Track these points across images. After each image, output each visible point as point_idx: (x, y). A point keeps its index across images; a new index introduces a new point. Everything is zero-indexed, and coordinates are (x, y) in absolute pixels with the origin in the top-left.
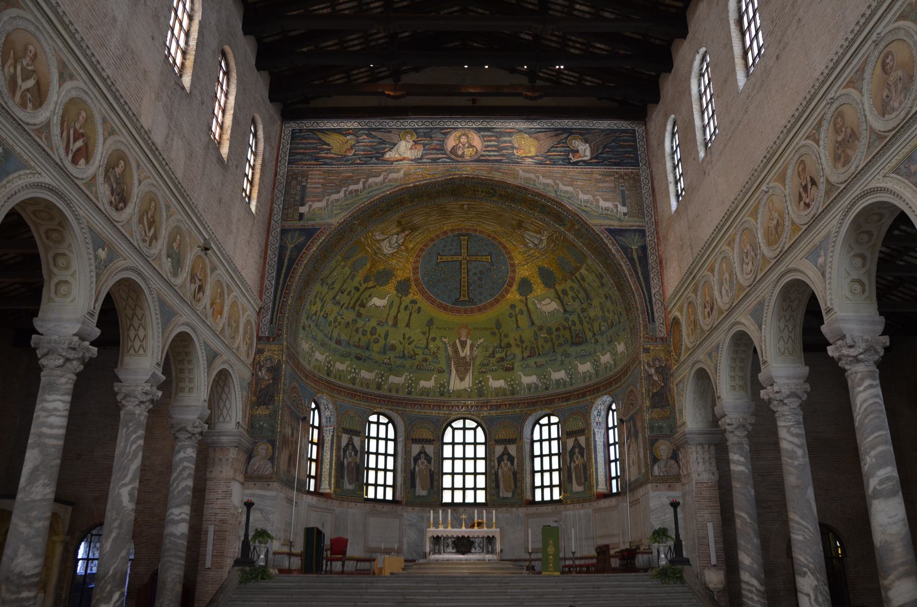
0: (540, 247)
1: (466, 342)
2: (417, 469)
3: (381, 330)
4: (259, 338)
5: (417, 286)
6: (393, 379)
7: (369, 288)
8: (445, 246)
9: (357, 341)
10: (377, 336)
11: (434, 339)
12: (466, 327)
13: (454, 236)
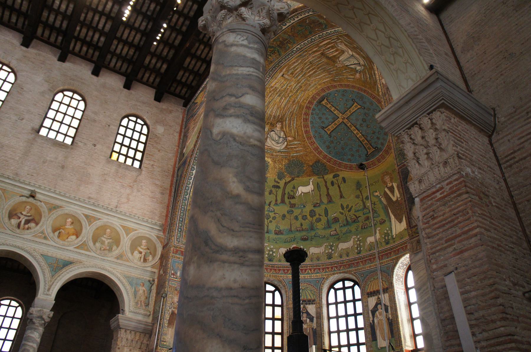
0: (362, 62)
1: (392, 187)
2: (376, 321)
3: (319, 210)
4: (164, 247)
5: (329, 162)
6: (343, 246)
7: (289, 182)
8: (320, 118)
9: (298, 225)
10: (317, 216)
11: (367, 198)
12: (386, 173)
13: (317, 106)
